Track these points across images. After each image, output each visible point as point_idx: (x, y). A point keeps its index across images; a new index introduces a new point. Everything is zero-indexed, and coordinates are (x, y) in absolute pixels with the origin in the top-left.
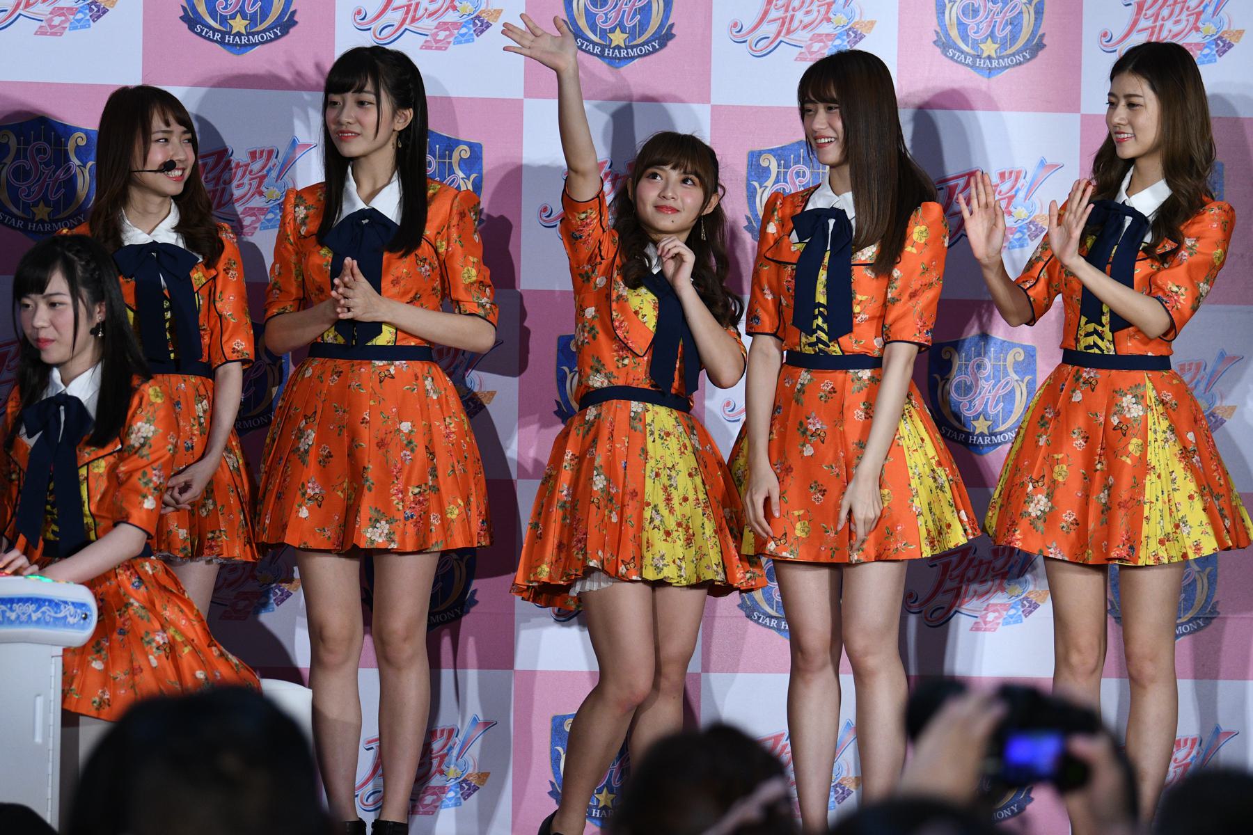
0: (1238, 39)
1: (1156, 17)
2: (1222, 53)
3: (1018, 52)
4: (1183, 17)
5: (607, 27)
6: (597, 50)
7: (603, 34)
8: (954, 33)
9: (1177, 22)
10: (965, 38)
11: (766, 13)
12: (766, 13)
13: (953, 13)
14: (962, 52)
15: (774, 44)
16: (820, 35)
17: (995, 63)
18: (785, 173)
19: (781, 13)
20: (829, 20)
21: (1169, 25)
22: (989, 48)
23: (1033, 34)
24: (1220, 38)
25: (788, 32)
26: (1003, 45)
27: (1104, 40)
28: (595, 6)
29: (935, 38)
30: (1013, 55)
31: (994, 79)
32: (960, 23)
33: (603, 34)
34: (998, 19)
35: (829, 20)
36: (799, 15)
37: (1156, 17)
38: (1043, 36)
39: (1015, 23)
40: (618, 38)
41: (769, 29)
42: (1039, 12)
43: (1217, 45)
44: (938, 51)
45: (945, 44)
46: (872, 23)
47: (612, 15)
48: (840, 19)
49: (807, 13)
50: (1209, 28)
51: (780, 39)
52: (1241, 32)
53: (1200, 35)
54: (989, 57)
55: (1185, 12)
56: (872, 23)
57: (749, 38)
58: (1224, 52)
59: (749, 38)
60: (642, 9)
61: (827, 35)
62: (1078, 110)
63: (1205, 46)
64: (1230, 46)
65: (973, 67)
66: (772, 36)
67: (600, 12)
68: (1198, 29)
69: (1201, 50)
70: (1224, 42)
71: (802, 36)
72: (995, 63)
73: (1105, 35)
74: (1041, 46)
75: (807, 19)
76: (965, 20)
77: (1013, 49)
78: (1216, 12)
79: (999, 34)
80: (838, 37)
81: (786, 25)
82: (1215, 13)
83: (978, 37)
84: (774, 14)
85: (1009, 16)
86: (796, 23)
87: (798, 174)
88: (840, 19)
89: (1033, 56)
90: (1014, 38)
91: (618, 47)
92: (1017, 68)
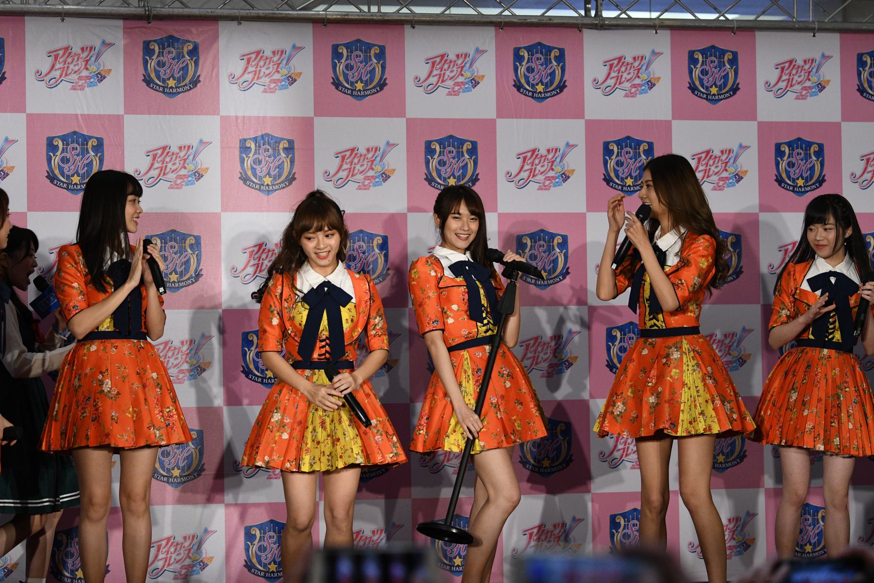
1: (351, 163)
3: (282, 182)
4: (365, 163)
5: (70, 173)
6: (65, 186)
7: (68, 177)
8: (249, 173)
9: (362, 165)
10: (255, 175)
11: (152, 164)
12: (152, 164)
13: (248, 162)
14: (254, 182)
17: (271, 188)
19: (160, 165)
20: (185, 168)
21: (358, 167)
22: (268, 180)
23: (290, 173)
25: (164, 174)
26: (275, 179)
28: (63, 163)
31: (270, 196)
32: (252, 168)
33: (68, 177)
34: (271, 165)
35: (185, 168)
36: (170, 166)
37: (351, 163)
39: (280, 167)
40: (76, 179)
41: (154, 173)
42: (292, 162)
44: (242, 182)
45: (245, 179)
46: (207, 169)
47: (72, 167)
48: (191, 167)
49: (174, 164)
50: (378, 168)
52: (394, 170)
54: (268, 185)
55: (366, 161)
56: (207, 169)
57: (144, 178)
59: (144, 178)
60: (88, 164)
64: (389, 177)
65: (260, 190)
66: (156, 177)
67: (66, 166)
68: (372, 169)
71: (171, 176)
72: (271, 188)
74: (294, 179)
75: (174, 167)
76: (255, 166)
77: (280, 181)
78: (381, 160)
79: (272, 173)
80: (189, 176)
81: (163, 171)
82: (381, 160)
83: (262, 175)
84: (156, 165)
85: (277, 164)
86: (168, 170)
87: (171, 247)
88: (191, 167)
89: (290, 183)
90: (280, 175)
91: (76, 184)
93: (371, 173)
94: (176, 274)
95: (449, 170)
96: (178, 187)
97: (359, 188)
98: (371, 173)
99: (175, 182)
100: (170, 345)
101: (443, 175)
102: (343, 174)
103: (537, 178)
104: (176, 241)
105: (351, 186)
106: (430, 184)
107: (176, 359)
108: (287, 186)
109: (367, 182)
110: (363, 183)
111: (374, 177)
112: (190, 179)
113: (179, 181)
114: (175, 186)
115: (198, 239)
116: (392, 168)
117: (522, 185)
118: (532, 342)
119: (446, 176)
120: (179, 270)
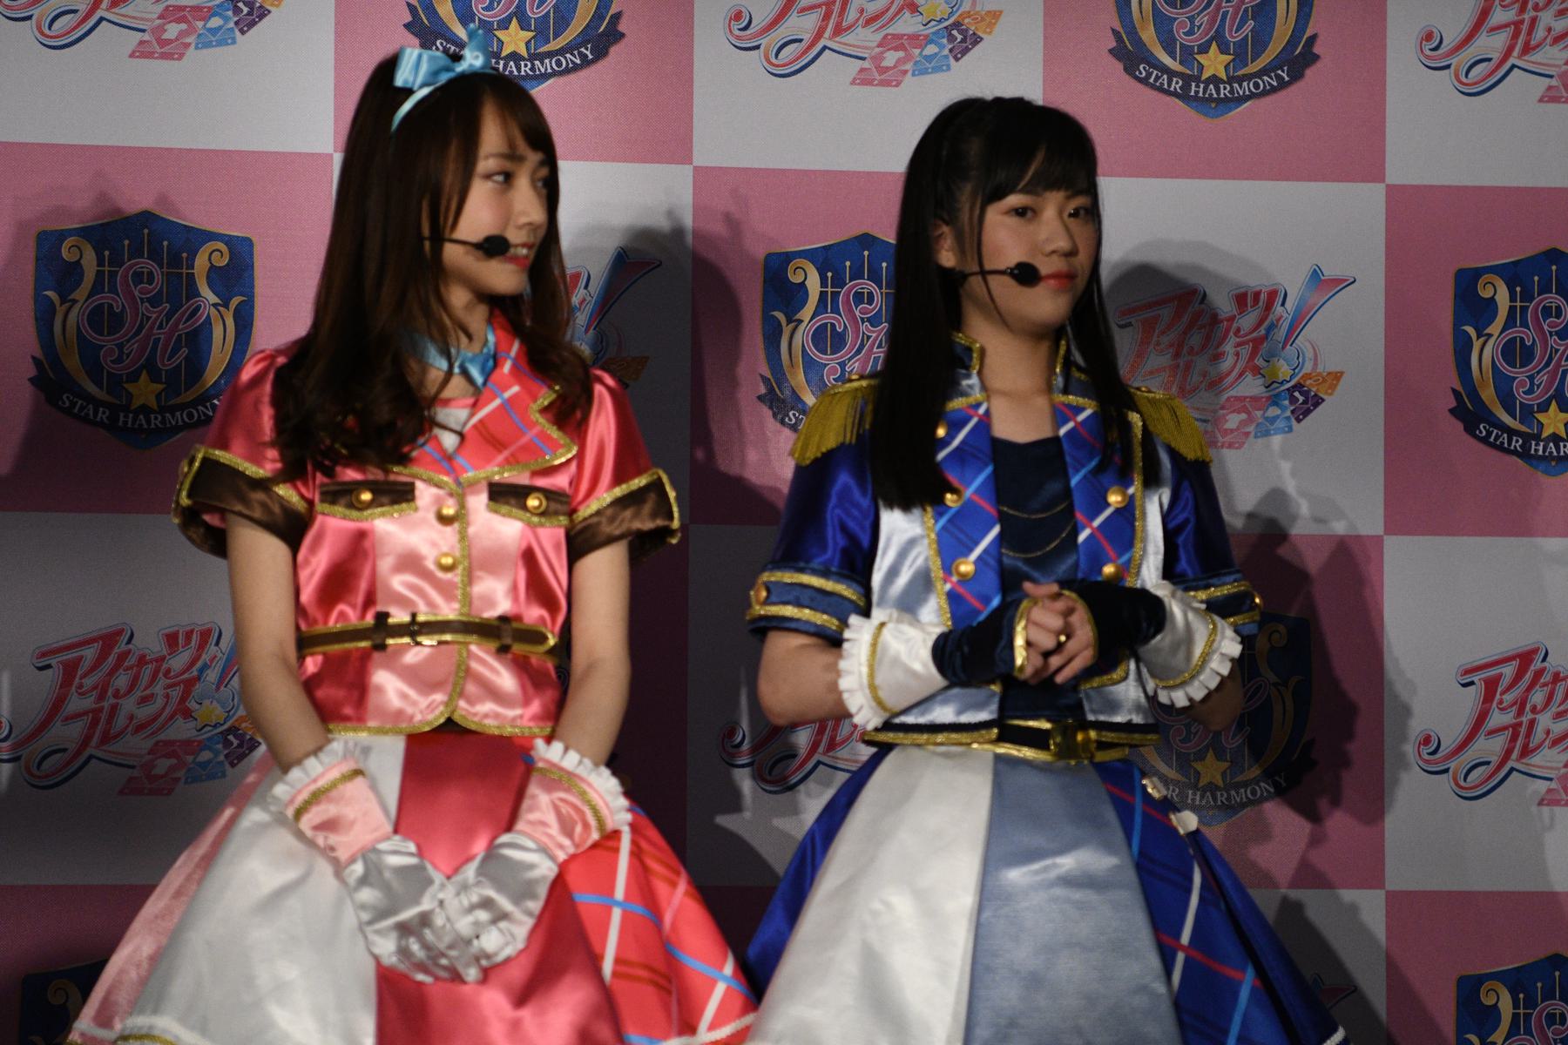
0: (991, 25)
15: (88, 24)
18: (113, 275)
23: (598, 16)
24: (957, 25)
27: (736, 26)
30: (561, 52)
38: (617, 17)
43: (951, 38)
51: (99, 13)
61: (196, 9)
62: (686, 158)
64: (977, 40)
69: (922, 48)
70: (964, 32)
73: (738, 16)
74: (613, 35)
87: (138, 277)
89: (601, 53)
92: (572, 77)
93: (907, 24)
96: (170, 51)
97: (863, 79)
98: (907, 24)
99: (161, 29)
101: (1181, 37)
102: (801, 25)
103: (1537, 57)
104: (155, 255)
105: (833, 72)
106: (1130, 70)
107: (144, 700)
108: (586, 63)
109: (891, 58)
110: (877, 59)
112: (215, 22)
116: (988, 7)
117: (1480, 84)
118: (1508, 671)
119: (1193, 41)
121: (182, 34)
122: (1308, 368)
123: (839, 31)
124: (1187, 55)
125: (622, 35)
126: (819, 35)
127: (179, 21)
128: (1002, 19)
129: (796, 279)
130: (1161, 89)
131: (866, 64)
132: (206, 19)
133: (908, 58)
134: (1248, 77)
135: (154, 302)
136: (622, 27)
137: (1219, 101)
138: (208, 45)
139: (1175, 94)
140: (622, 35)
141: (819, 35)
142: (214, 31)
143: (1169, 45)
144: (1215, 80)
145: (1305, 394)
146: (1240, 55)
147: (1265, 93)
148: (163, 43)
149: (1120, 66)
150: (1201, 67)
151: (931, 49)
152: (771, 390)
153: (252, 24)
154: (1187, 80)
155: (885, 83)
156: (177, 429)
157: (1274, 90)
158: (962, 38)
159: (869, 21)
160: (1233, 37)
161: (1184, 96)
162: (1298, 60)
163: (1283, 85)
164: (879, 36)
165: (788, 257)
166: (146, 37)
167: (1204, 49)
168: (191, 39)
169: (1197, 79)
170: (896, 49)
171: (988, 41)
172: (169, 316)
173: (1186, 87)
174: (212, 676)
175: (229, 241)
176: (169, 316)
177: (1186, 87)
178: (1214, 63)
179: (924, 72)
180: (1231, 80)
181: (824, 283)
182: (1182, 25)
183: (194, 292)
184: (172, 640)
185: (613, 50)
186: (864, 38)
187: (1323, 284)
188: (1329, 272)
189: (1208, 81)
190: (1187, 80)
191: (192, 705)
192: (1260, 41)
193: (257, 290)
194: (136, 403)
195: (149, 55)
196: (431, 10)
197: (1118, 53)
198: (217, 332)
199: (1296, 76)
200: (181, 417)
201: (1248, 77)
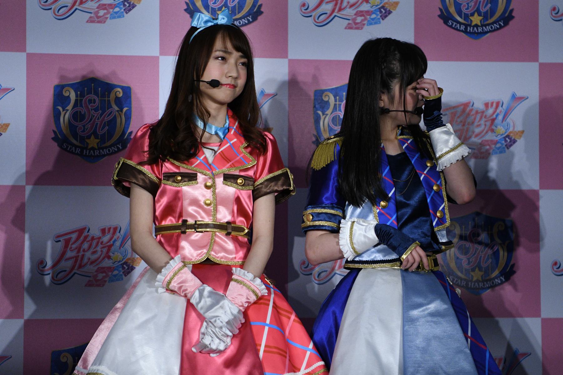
2: (384, 17)
15: (71, 11)
16: (105, 5)
23: (254, 5)
24: (383, 7)
27: (303, 9)
29: (186, 7)
38: (260, 6)
43: (381, 12)
53: (369, 5)
58: (386, 16)
61: (110, 5)
63: (372, 13)
64: (390, 12)
69: (370, 15)
73: (304, 5)
87: (90, 101)
89: (255, 19)
93: (365, 7)
94: (96, 137)
95: (472, 4)
96: (100, 20)
97: (349, 27)
98: (365, 7)
100: (85, 233)
101: (464, 10)
102: (327, 7)
104: (96, 93)
105: (338, 24)
106: (446, 23)
107: (94, 253)
109: (359, 19)
110: (354, 20)
111: (368, 13)
112: (117, 9)
113: (102, 13)
114: (96, 19)
115: (127, 91)
119: (469, 12)
120: (100, 133)
121: (105, 14)
122: (511, 129)
123: (340, 10)
124: (466, 17)
125: (262, 13)
126: (333, 11)
127: (104, 9)
128: (399, 5)
129: (326, 99)
130: (457, 29)
131: (350, 22)
132: (113, 8)
133: (365, 19)
134: (488, 25)
135: (96, 110)
136: (262, 10)
137: (478, 33)
138: (114, 18)
139: (462, 31)
140: (262, 13)
141: (333, 11)
142: (116, 13)
143: (460, 13)
144: (476, 26)
145: (510, 139)
146: (486, 16)
147: (495, 30)
148: (98, 17)
149: (441, 21)
150: (471, 21)
151: (374, 16)
152: (317, 140)
153: (130, 10)
154: (466, 26)
155: (357, 28)
156: (104, 156)
157: (498, 29)
158: (385, 12)
159: (352, 6)
160: (483, 10)
161: (465, 32)
162: (507, 18)
163: (501, 27)
164: (355, 12)
165: (323, 91)
166: (92, 15)
167: (472, 15)
168: (108, 16)
169: (470, 26)
170: (361, 16)
171: (394, 13)
172: (101, 115)
173: (466, 29)
174: (118, 243)
175: (123, 88)
176: (101, 115)
177: (466, 29)
178: (476, 20)
179: (371, 24)
180: (482, 26)
181: (336, 101)
182: (465, 6)
183: (110, 106)
184: (103, 231)
185: (259, 18)
186: (350, 12)
187: (517, 99)
188: (519, 94)
189: (474, 26)
190: (466, 26)
191: (111, 254)
192: (493, 12)
193: (132, 106)
194: (90, 147)
195: (93, 22)
196: (194, 4)
197: (441, 16)
198: (118, 120)
199: (506, 23)
200: (106, 151)
201: (488, 25)
